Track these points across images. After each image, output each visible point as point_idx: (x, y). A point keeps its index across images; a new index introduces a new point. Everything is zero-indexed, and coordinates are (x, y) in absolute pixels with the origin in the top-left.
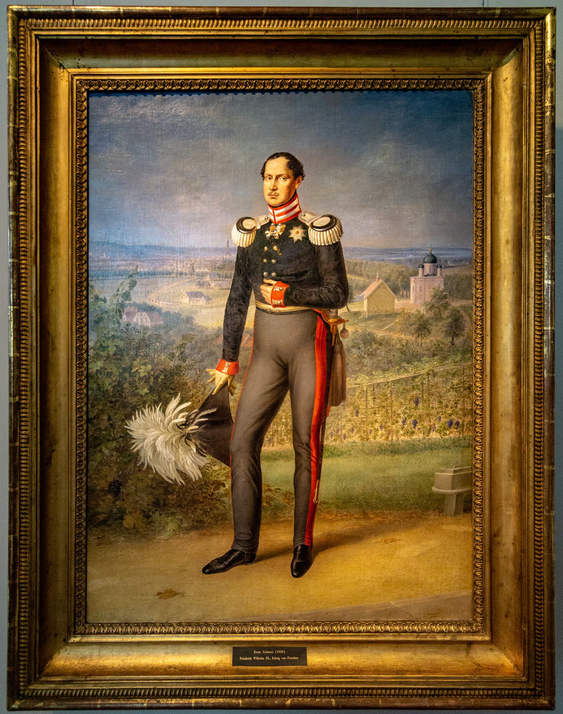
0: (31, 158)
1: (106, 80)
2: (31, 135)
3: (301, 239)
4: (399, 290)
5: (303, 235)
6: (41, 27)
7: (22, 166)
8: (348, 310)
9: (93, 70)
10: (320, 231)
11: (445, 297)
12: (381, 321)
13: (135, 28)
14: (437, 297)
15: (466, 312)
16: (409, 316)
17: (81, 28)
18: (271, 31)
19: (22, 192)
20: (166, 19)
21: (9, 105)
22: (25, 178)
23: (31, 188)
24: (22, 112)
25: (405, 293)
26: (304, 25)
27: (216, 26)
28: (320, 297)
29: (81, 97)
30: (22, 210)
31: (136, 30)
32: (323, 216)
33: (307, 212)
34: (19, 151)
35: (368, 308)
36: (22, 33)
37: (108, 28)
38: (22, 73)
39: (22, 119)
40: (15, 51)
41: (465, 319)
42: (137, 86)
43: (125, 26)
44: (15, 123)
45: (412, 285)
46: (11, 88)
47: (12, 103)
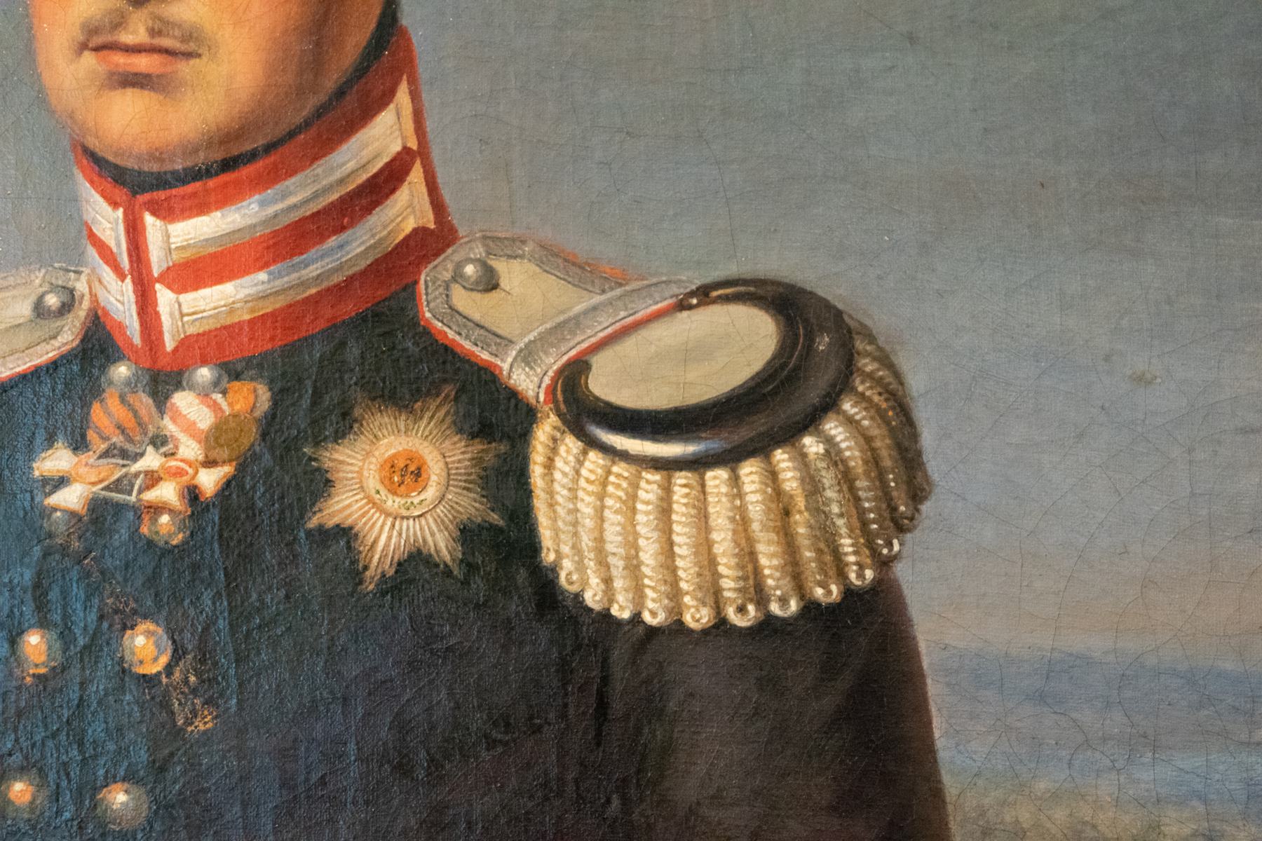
3: (441, 544)
5: (471, 506)
10: (658, 464)
32: (705, 295)
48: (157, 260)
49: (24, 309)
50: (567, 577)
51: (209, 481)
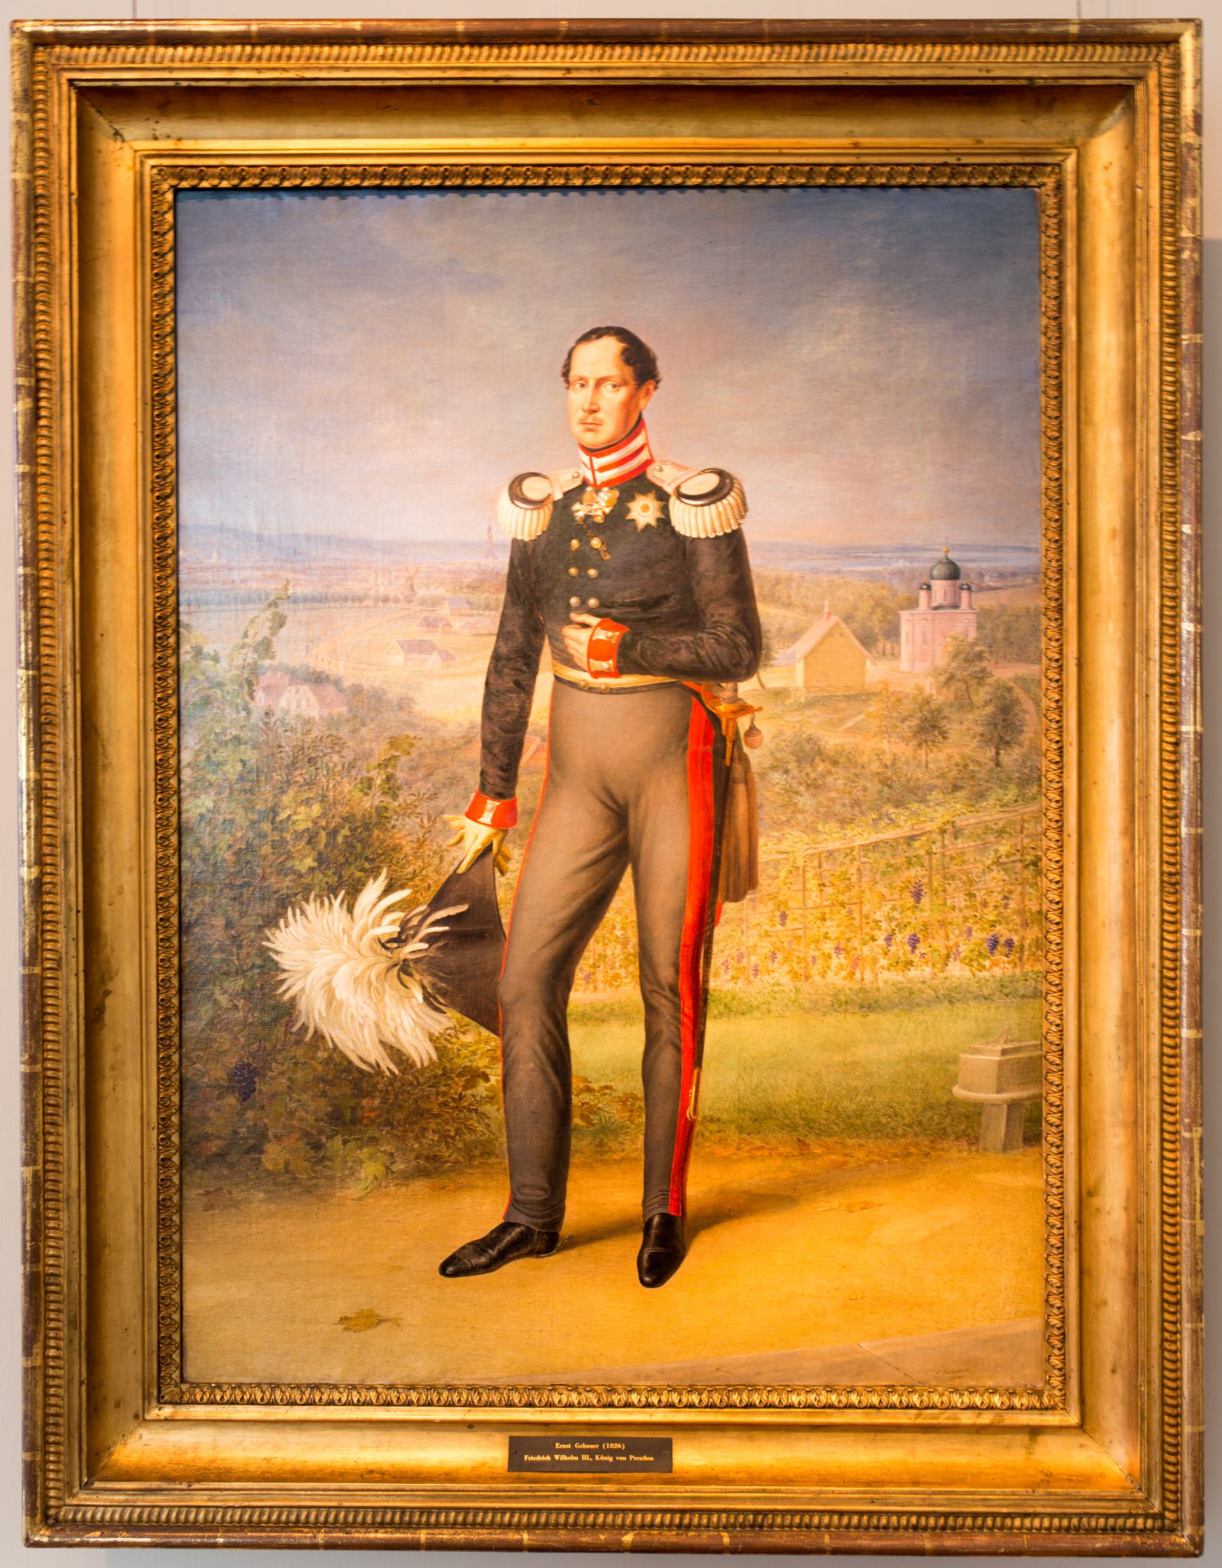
0: (61, 348)
1: (217, 167)
2: (61, 298)
3: (653, 523)
4: (876, 640)
6: (81, 65)
7: (42, 365)
8: (762, 685)
9: (187, 145)
11: (979, 656)
12: (836, 710)
13: (283, 64)
14: (962, 656)
15: (1027, 691)
16: (899, 700)
17: (167, 64)
18: (577, 69)
19: (43, 422)
20: (349, 45)
21: (16, 236)
22: (49, 390)
23: (62, 415)
24: (42, 249)
25: (888, 647)
26: (649, 58)
27: (459, 58)
28: (698, 655)
29: (161, 203)
30: (43, 460)
31: (284, 69)
32: (704, 471)
33: (664, 462)
34: (36, 332)
35: (806, 681)
36: (41, 78)
37: (225, 64)
38: (41, 163)
39: (42, 263)
40: (25, 117)
41: (1024, 707)
42: (283, 179)
43: (260, 59)
44: (28, 274)
45: (905, 628)
46: (21, 199)
47: (22, 230)
48: (596, 466)
49: (570, 477)
50: (677, 529)
51: (607, 510)
